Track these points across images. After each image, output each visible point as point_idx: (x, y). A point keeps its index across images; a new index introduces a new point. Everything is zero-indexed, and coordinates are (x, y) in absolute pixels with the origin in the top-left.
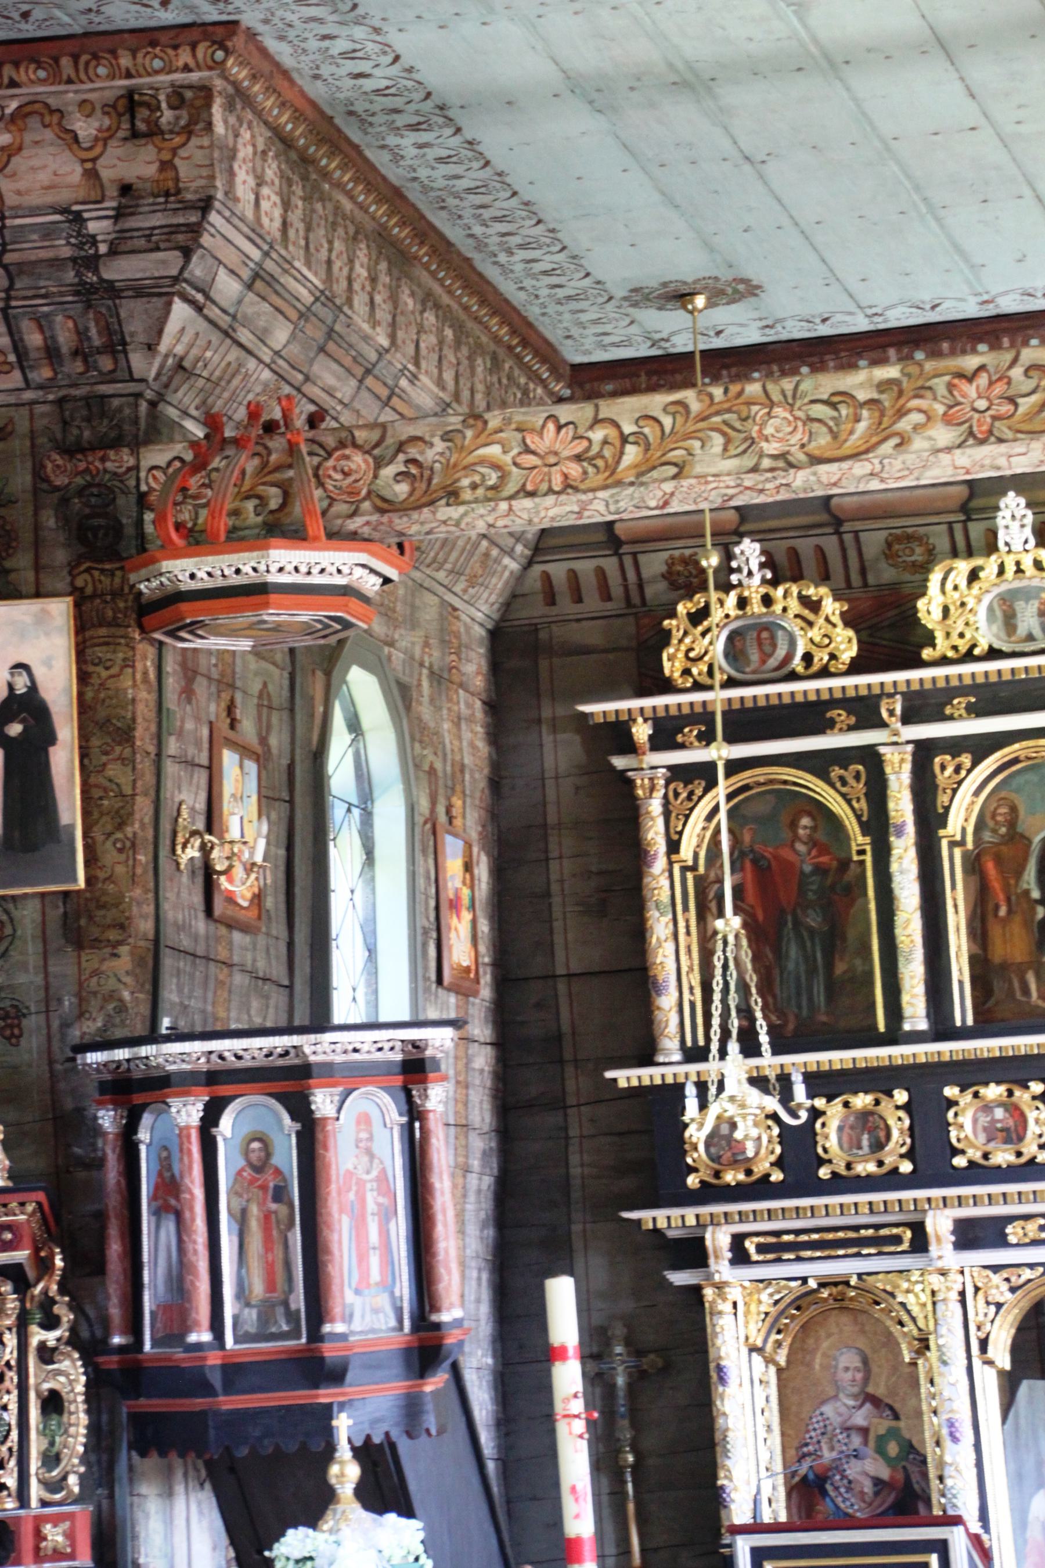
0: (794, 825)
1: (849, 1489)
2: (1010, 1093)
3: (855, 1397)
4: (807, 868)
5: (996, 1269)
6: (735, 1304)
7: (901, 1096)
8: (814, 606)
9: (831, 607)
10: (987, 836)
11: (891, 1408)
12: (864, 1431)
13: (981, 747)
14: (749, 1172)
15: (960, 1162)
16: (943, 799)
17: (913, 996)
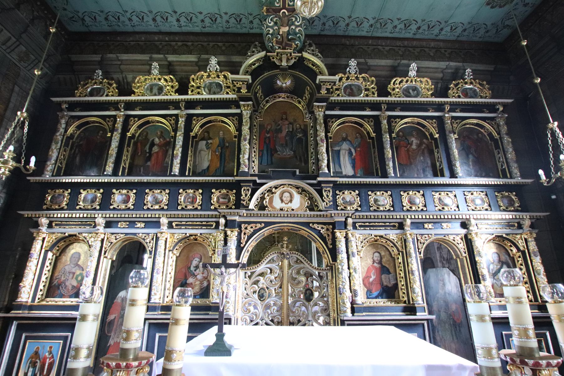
0: (98, 132)
1: (65, 288)
2: (128, 192)
3: (74, 264)
4: (98, 142)
5: (113, 234)
6: (44, 239)
7: (101, 191)
8: (111, 85)
9: (114, 85)
10: (140, 138)
11: (82, 268)
12: (74, 273)
13: (141, 117)
14: (59, 206)
15: (112, 207)
16: (130, 127)
17: (109, 167)
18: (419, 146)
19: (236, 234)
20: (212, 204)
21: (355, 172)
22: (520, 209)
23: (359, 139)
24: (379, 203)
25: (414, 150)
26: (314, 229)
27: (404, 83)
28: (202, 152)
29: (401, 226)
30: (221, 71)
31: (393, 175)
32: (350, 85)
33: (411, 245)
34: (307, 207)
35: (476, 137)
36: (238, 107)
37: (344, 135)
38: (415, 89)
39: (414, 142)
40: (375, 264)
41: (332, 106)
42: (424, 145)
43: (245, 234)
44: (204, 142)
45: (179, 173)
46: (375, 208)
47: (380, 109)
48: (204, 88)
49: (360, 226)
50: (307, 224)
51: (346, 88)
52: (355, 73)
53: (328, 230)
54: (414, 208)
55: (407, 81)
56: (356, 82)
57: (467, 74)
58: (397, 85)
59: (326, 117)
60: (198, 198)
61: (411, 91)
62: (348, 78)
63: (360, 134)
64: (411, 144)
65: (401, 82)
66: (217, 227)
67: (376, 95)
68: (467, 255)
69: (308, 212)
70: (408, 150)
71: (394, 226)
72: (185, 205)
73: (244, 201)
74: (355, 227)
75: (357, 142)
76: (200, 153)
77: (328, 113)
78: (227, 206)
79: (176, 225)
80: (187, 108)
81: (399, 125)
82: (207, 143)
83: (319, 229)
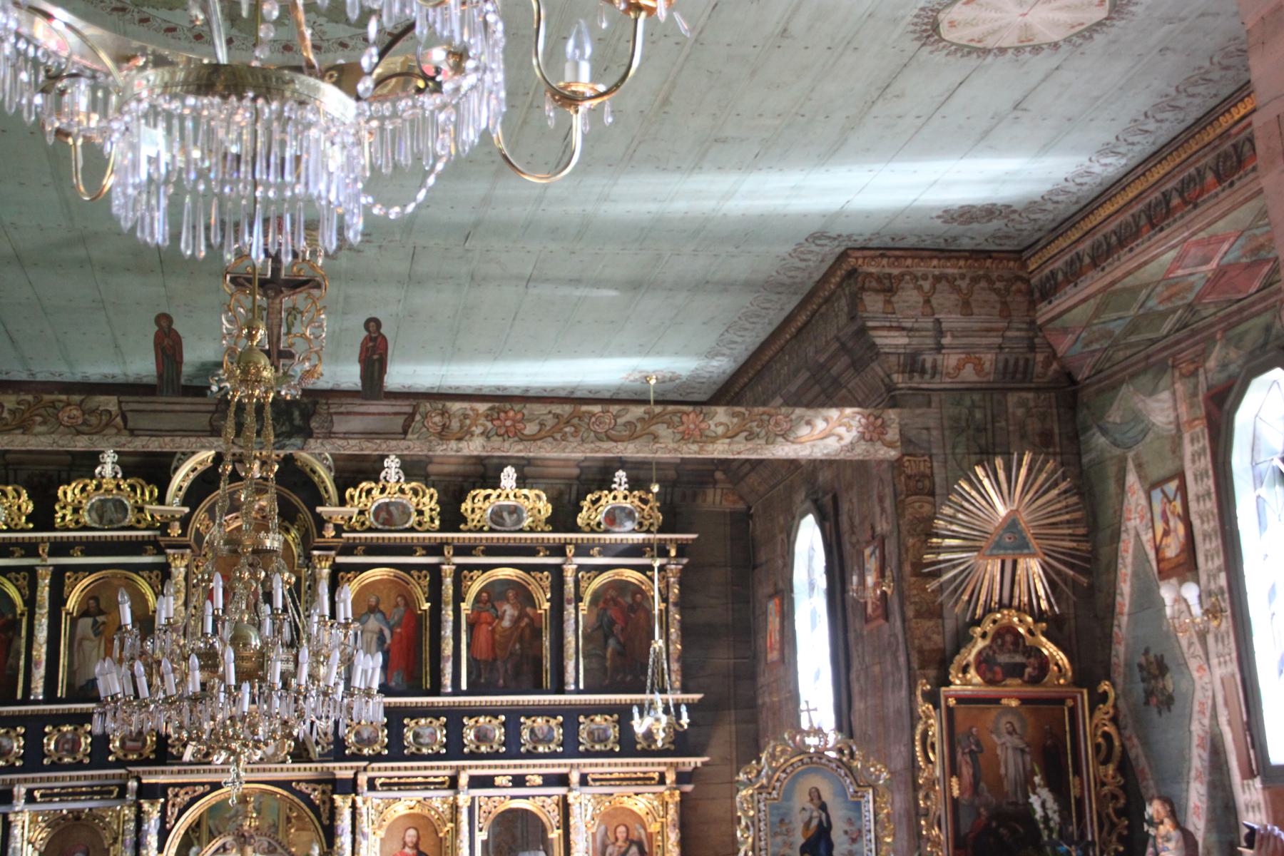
18: (516, 621)
19: (159, 807)
20: (111, 753)
21: (386, 679)
22: (672, 747)
23: (402, 608)
24: (422, 740)
25: (505, 630)
26: (300, 794)
27: (493, 498)
28: (87, 644)
29: (453, 783)
30: (124, 478)
31: (449, 690)
32: (387, 504)
33: (464, 817)
34: (288, 753)
35: (629, 600)
36: (160, 551)
37: (373, 600)
38: (515, 510)
39: (508, 612)
40: (407, 850)
41: (348, 549)
42: (526, 620)
43: (173, 805)
44: (88, 621)
45: (45, 693)
46: (413, 749)
47: (441, 554)
48: (89, 511)
49: (383, 785)
50: (285, 784)
51: (379, 508)
52: (398, 481)
53: (324, 792)
54: (483, 749)
55: (499, 496)
56: (396, 498)
57: (616, 480)
58: (478, 505)
59: (336, 570)
60: (82, 740)
61: (505, 515)
62: (383, 490)
63: (405, 598)
64: (502, 618)
65: (487, 497)
66: (122, 794)
67: (437, 522)
68: (560, 831)
69: (289, 764)
70: (493, 631)
71: (443, 783)
72: (59, 755)
73: (173, 747)
74: (372, 785)
75: (397, 615)
76: (80, 644)
77: (340, 560)
78: (141, 755)
79: (42, 796)
80: (52, 554)
81: (476, 585)
82: (95, 622)
83: (309, 791)
